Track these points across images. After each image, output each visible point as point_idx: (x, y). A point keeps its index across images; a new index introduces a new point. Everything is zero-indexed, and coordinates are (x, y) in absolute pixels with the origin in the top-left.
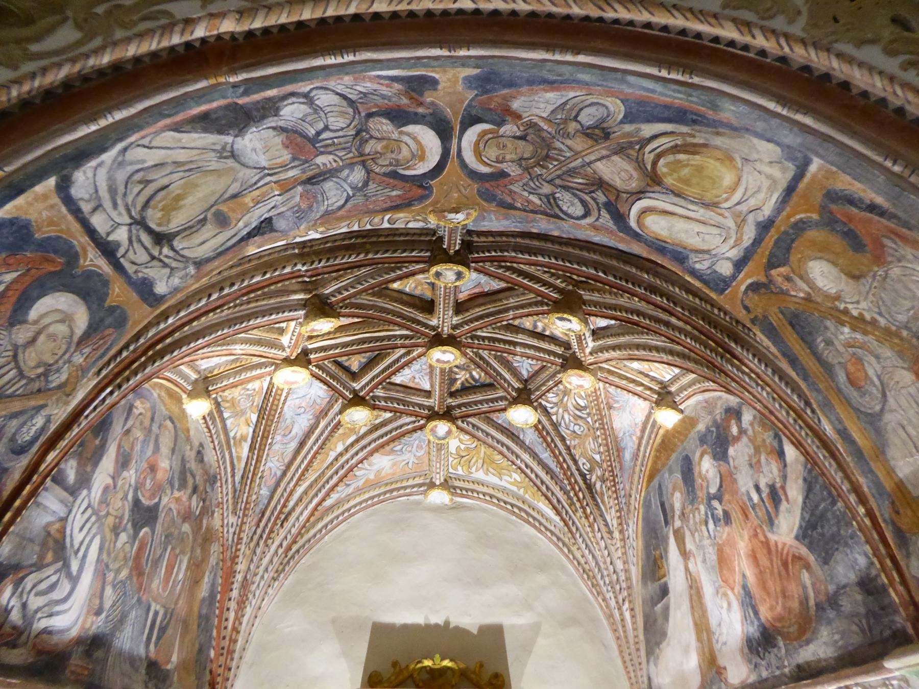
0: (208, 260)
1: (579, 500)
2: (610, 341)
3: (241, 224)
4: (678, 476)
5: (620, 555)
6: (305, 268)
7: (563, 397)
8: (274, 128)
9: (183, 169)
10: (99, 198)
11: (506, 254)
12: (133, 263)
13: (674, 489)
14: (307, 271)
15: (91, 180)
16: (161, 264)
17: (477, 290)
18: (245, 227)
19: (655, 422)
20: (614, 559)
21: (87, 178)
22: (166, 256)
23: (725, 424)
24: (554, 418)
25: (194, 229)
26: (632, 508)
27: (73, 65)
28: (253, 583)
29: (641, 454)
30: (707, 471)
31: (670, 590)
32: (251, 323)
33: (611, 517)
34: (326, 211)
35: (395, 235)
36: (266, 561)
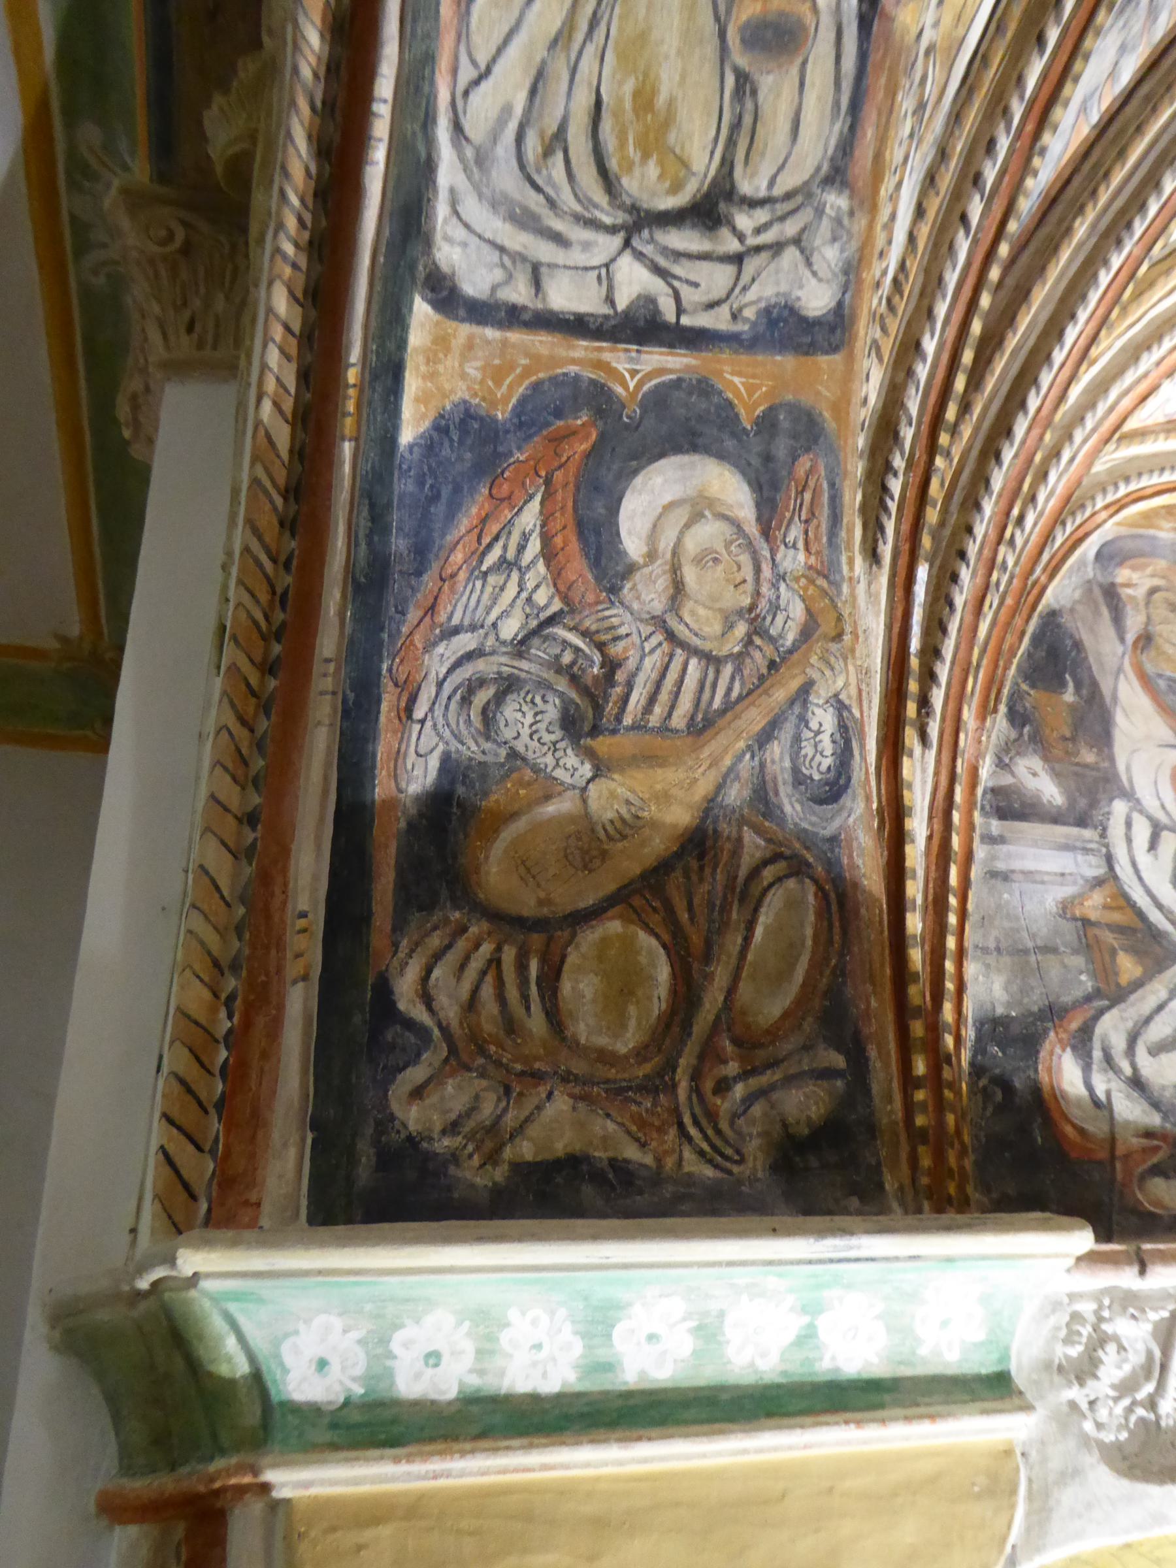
0: (847, 146)
9: (579, 36)
10: (519, 257)
12: (711, 305)
15: (474, 241)
16: (764, 255)
21: (464, 245)
22: (758, 231)
25: (748, 120)
27: (297, 112)
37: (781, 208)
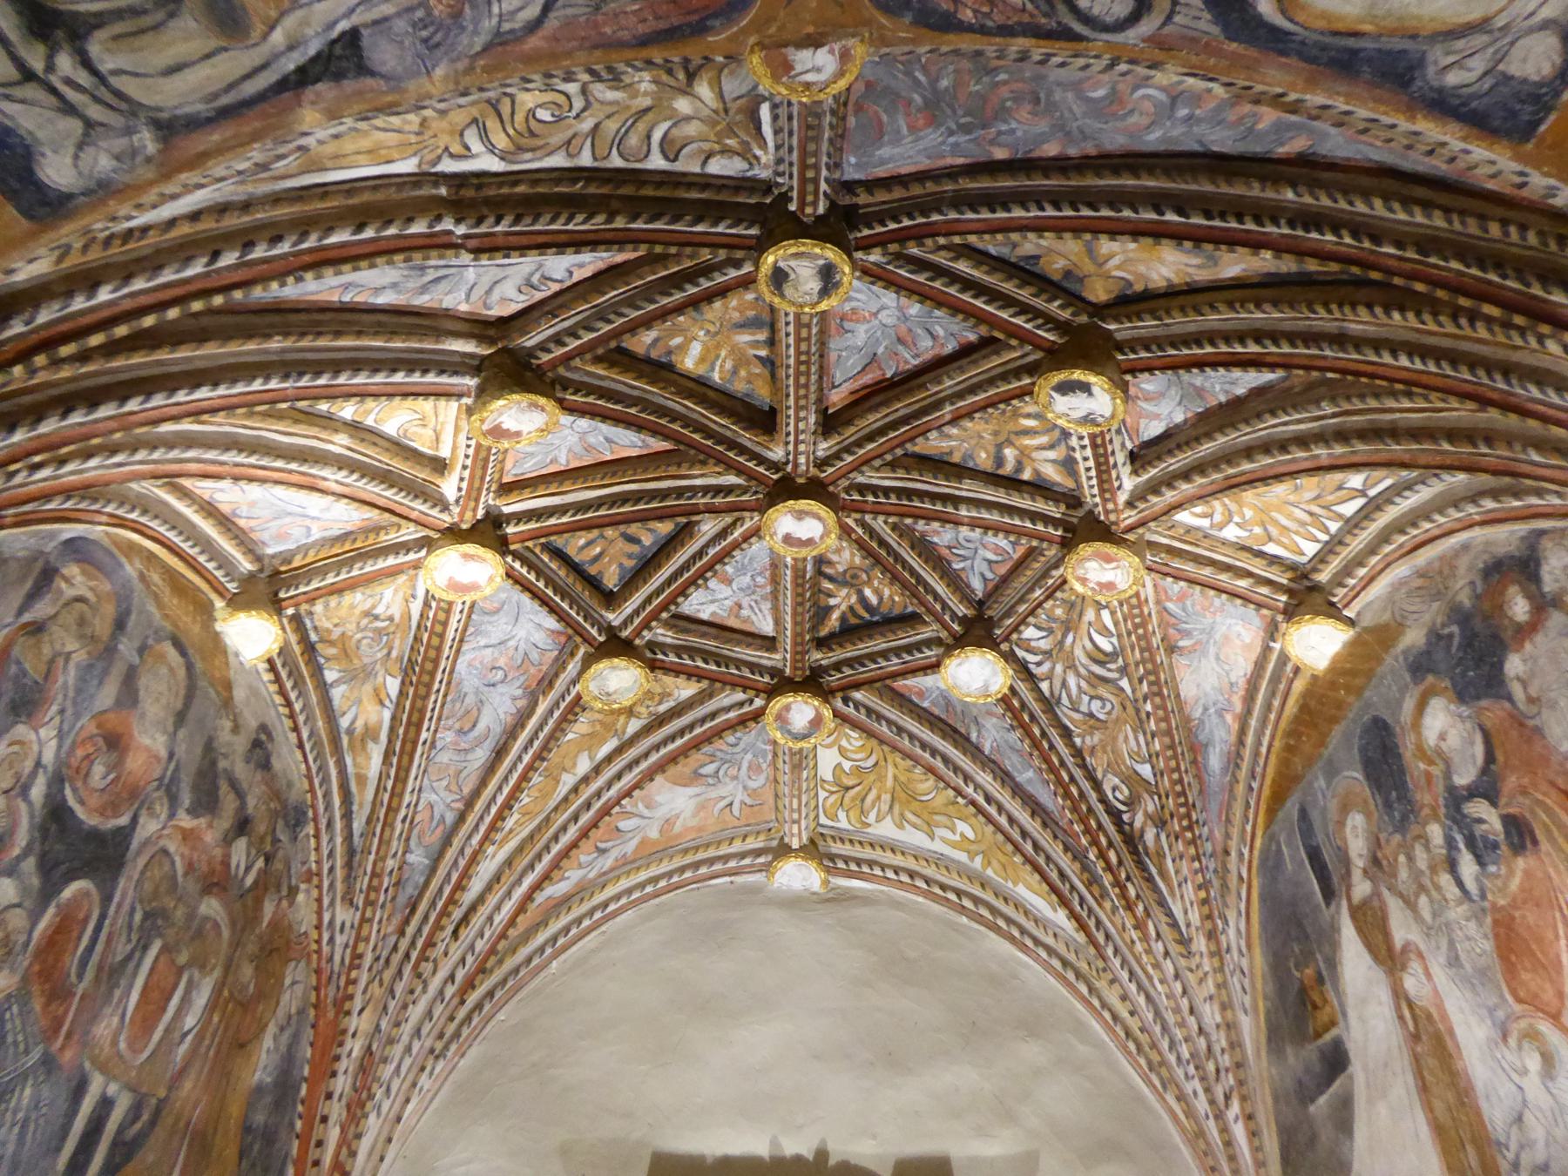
0: (194, 124)
1: (1109, 868)
2: (1175, 463)
3: (278, 37)
4: (1354, 777)
5: (1212, 990)
6: (461, 230)
7: (1064, 636)
11: (935, 217)
13: (1345, 809)
14: (466, 237)
17: (868, 378)
18: (291, 48)
19: (1284, 659)
20: (1198, 1002)
23: (1486, 606)
24: (1044, 686)
25: (147, 21)
26: (1233, 881)
28: (385, 1060)
29: (1247, 753)
30: (1442, 737)
31: (1352, 1055)
32: (342, 380)
33: (1185, 906)
34: (498, 33)
35: (677, 185)
36: (416, 1013)
37: (103, 93)
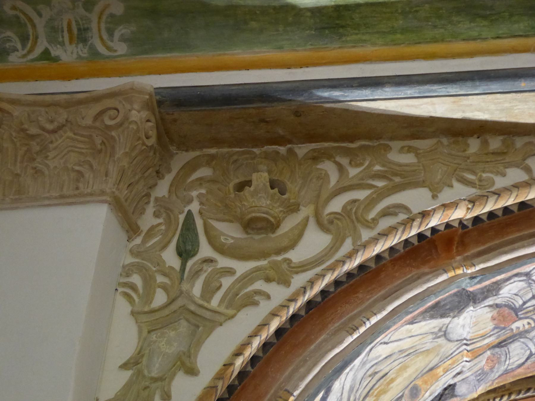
8: (490, 306)
15: (342, 385)
34: (506, 370)
